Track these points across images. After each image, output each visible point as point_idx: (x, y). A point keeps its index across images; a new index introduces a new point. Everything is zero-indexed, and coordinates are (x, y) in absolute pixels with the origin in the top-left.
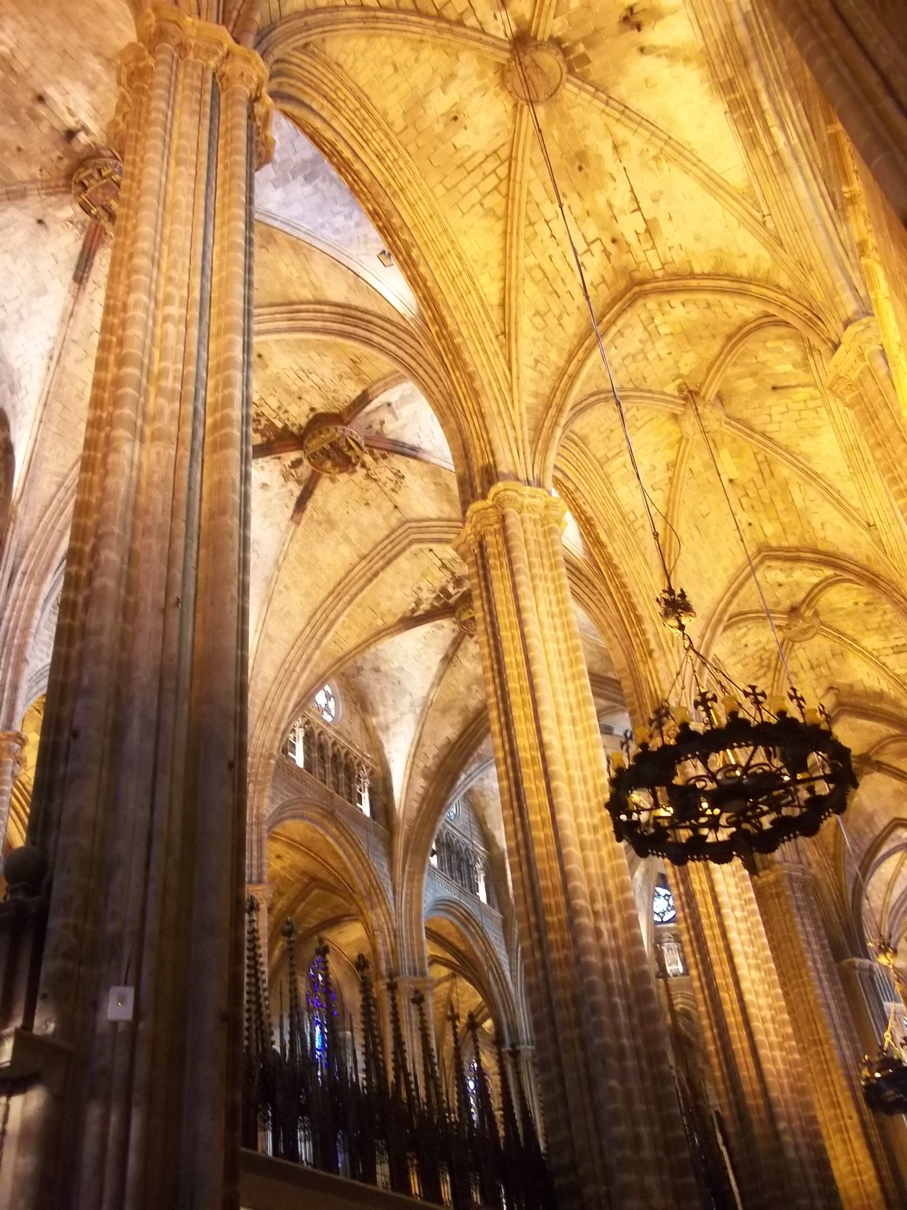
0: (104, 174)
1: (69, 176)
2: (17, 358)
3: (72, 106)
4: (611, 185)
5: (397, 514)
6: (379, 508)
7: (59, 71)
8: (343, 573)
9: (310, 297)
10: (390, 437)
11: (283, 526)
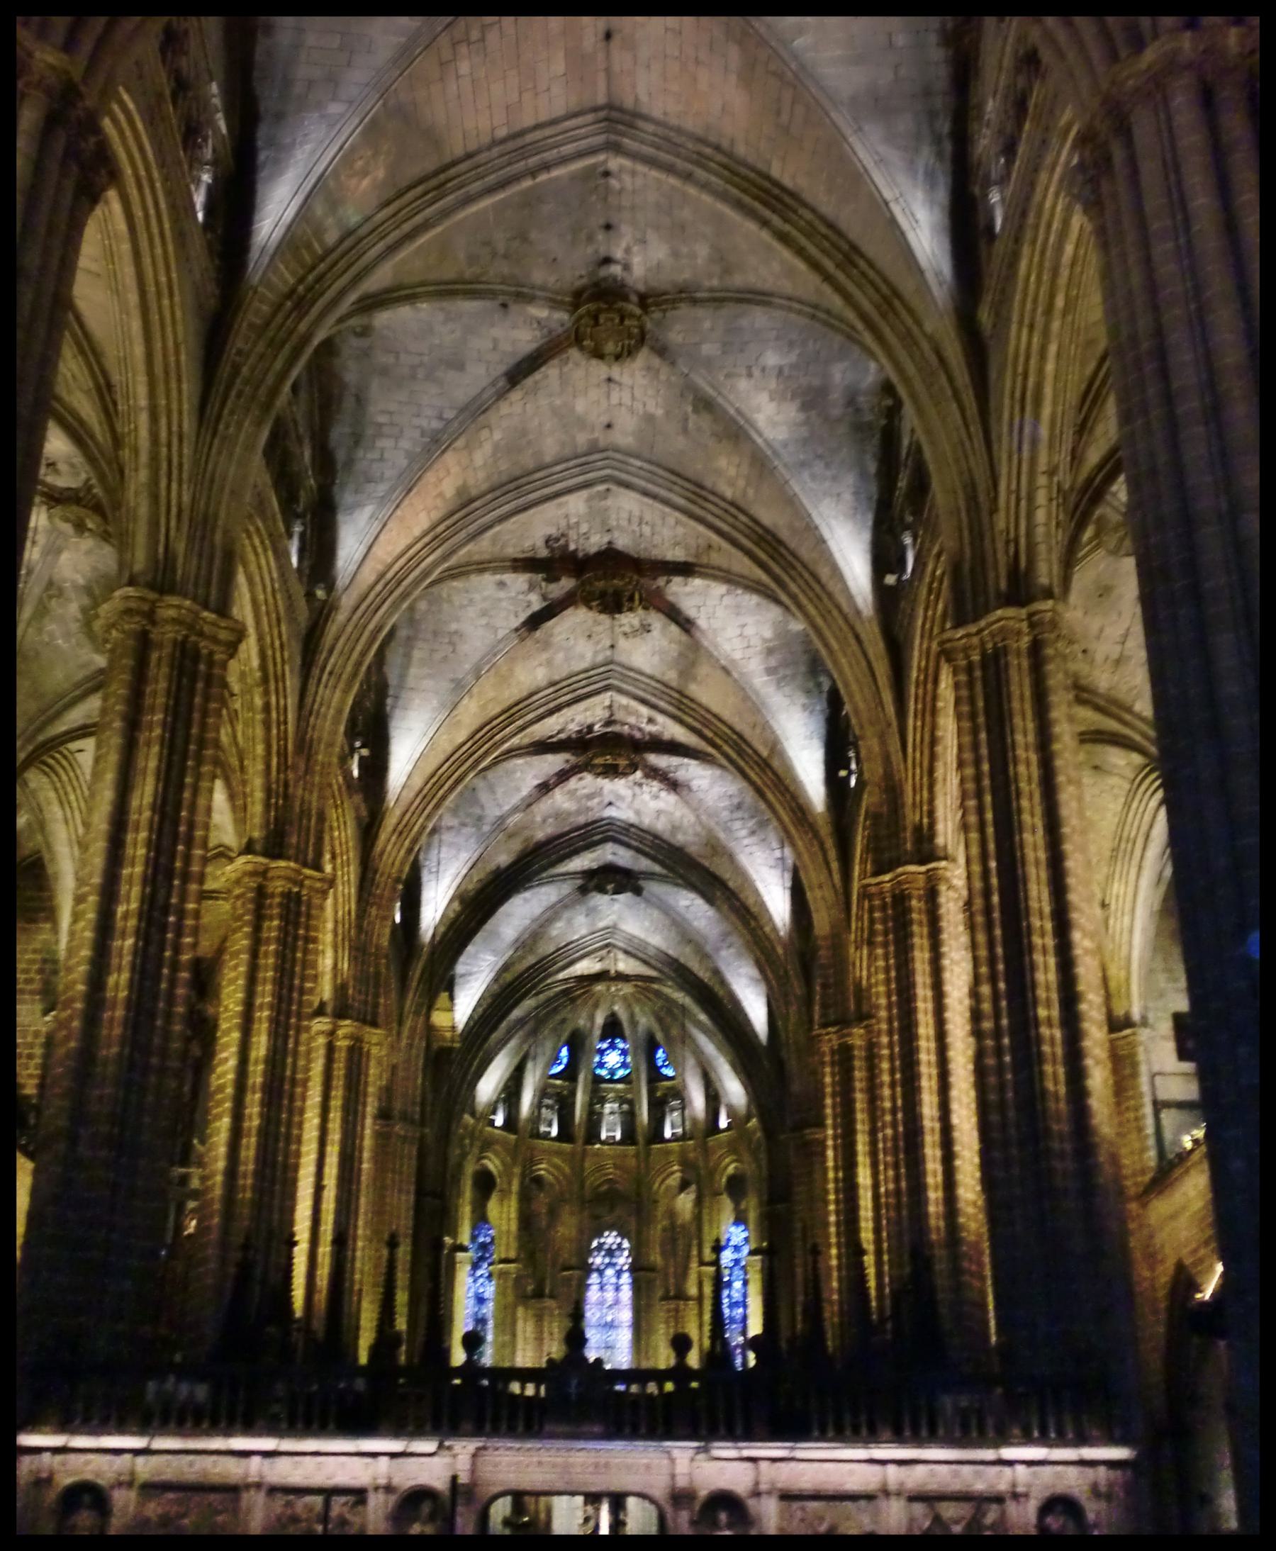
0: (627, 322)
1: (578, 294)
2: (383, 412)
3: (635, 249)
4: (1114, 617)
5: (608, 653)
6: (598, 643)
7: (657, 228)
8: (525, 694)
9: (729, 493)
10: (671, 598)
11: (501, 633)
